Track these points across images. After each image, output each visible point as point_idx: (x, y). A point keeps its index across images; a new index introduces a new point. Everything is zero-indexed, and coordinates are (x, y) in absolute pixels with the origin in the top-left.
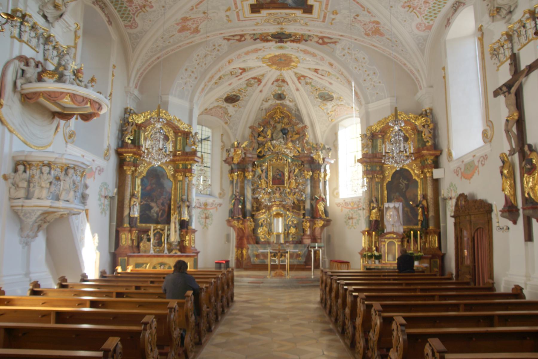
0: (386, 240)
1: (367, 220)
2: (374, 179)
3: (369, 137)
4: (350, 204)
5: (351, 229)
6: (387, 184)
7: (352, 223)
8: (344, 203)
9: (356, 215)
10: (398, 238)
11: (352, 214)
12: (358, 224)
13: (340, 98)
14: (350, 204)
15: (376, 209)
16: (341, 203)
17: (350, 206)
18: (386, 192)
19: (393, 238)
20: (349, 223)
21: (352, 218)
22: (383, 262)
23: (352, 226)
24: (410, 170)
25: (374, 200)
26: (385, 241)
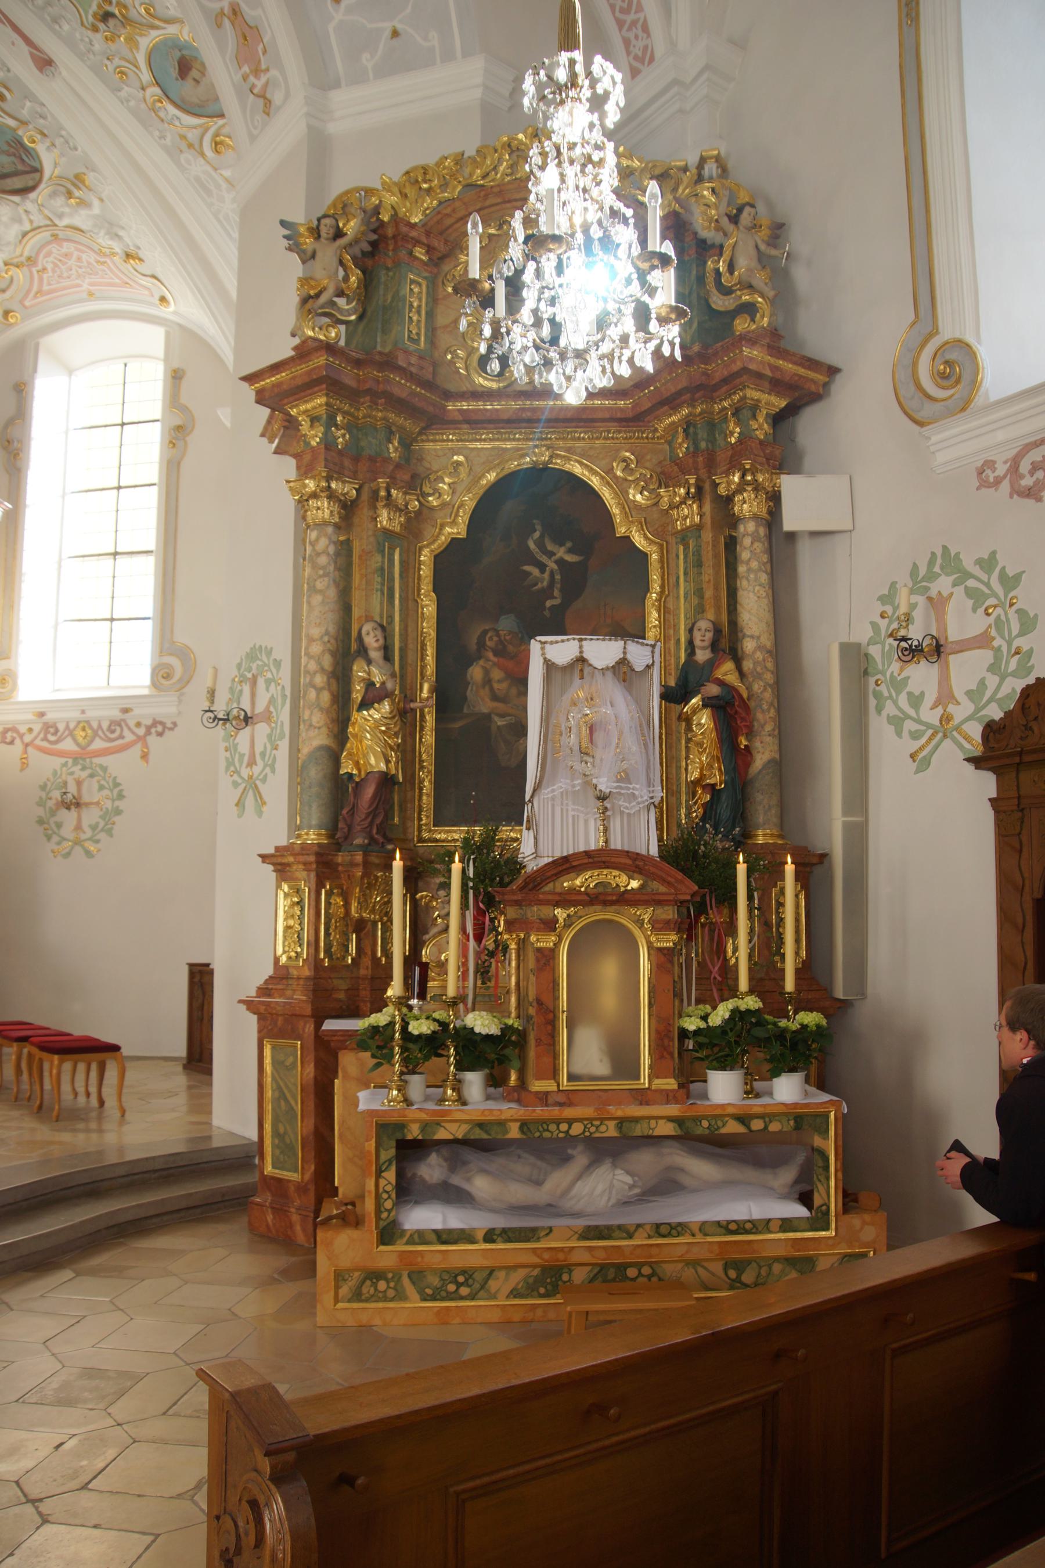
0: (560, 913)
1: (316, 773)
2: (365, 512)
3: (356, 241)
4: (71, 734)
5: (68, 854)
6: (438, 559)
7: (78, 827)
8: (37, 728)
9: (101, 788)
10: (657, 902)
11: (79, 783)
12: (109, 833)
13: (79, 180)
14: (71, 734)
15: (386, 706)
16: (23, 729)
17: (68, 745)
18: (429, 607)
19: (624, 899)
20: (59, 825)
21: (78, 805)
22: (538, 1086)
23: (77, 842)
24: (595, 482)
25: (372, 640)
26: (550, 925)
